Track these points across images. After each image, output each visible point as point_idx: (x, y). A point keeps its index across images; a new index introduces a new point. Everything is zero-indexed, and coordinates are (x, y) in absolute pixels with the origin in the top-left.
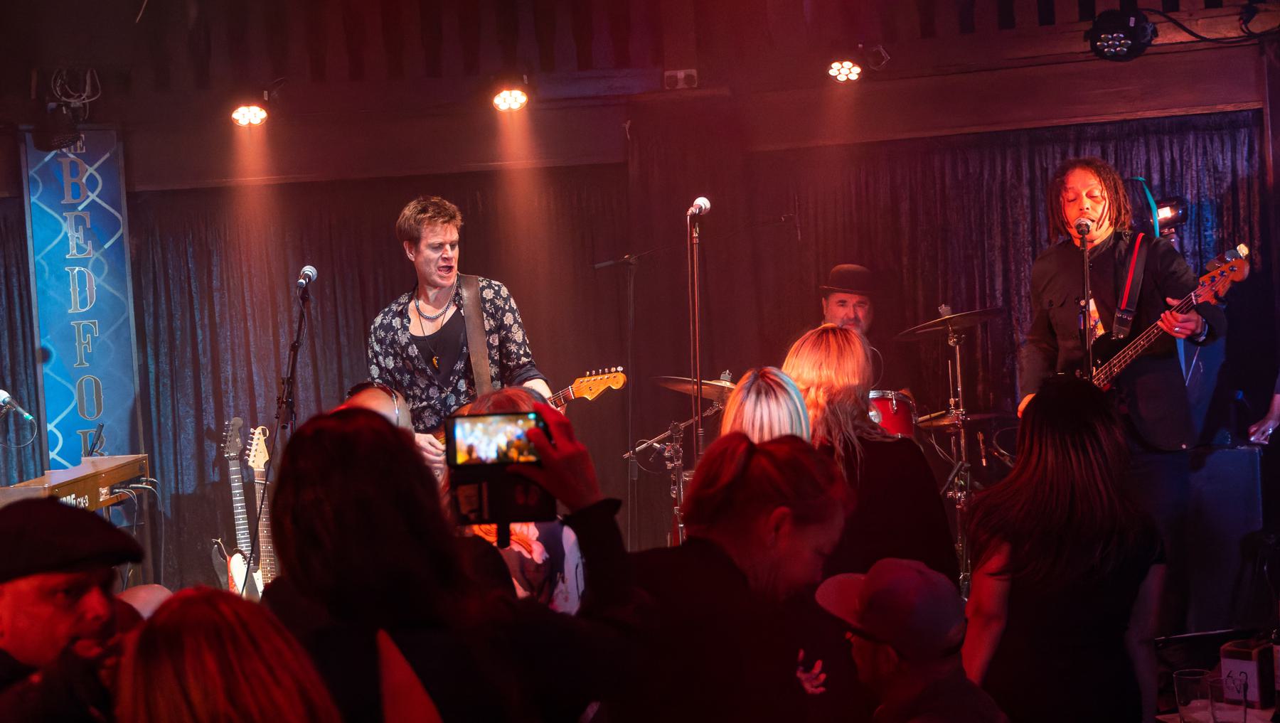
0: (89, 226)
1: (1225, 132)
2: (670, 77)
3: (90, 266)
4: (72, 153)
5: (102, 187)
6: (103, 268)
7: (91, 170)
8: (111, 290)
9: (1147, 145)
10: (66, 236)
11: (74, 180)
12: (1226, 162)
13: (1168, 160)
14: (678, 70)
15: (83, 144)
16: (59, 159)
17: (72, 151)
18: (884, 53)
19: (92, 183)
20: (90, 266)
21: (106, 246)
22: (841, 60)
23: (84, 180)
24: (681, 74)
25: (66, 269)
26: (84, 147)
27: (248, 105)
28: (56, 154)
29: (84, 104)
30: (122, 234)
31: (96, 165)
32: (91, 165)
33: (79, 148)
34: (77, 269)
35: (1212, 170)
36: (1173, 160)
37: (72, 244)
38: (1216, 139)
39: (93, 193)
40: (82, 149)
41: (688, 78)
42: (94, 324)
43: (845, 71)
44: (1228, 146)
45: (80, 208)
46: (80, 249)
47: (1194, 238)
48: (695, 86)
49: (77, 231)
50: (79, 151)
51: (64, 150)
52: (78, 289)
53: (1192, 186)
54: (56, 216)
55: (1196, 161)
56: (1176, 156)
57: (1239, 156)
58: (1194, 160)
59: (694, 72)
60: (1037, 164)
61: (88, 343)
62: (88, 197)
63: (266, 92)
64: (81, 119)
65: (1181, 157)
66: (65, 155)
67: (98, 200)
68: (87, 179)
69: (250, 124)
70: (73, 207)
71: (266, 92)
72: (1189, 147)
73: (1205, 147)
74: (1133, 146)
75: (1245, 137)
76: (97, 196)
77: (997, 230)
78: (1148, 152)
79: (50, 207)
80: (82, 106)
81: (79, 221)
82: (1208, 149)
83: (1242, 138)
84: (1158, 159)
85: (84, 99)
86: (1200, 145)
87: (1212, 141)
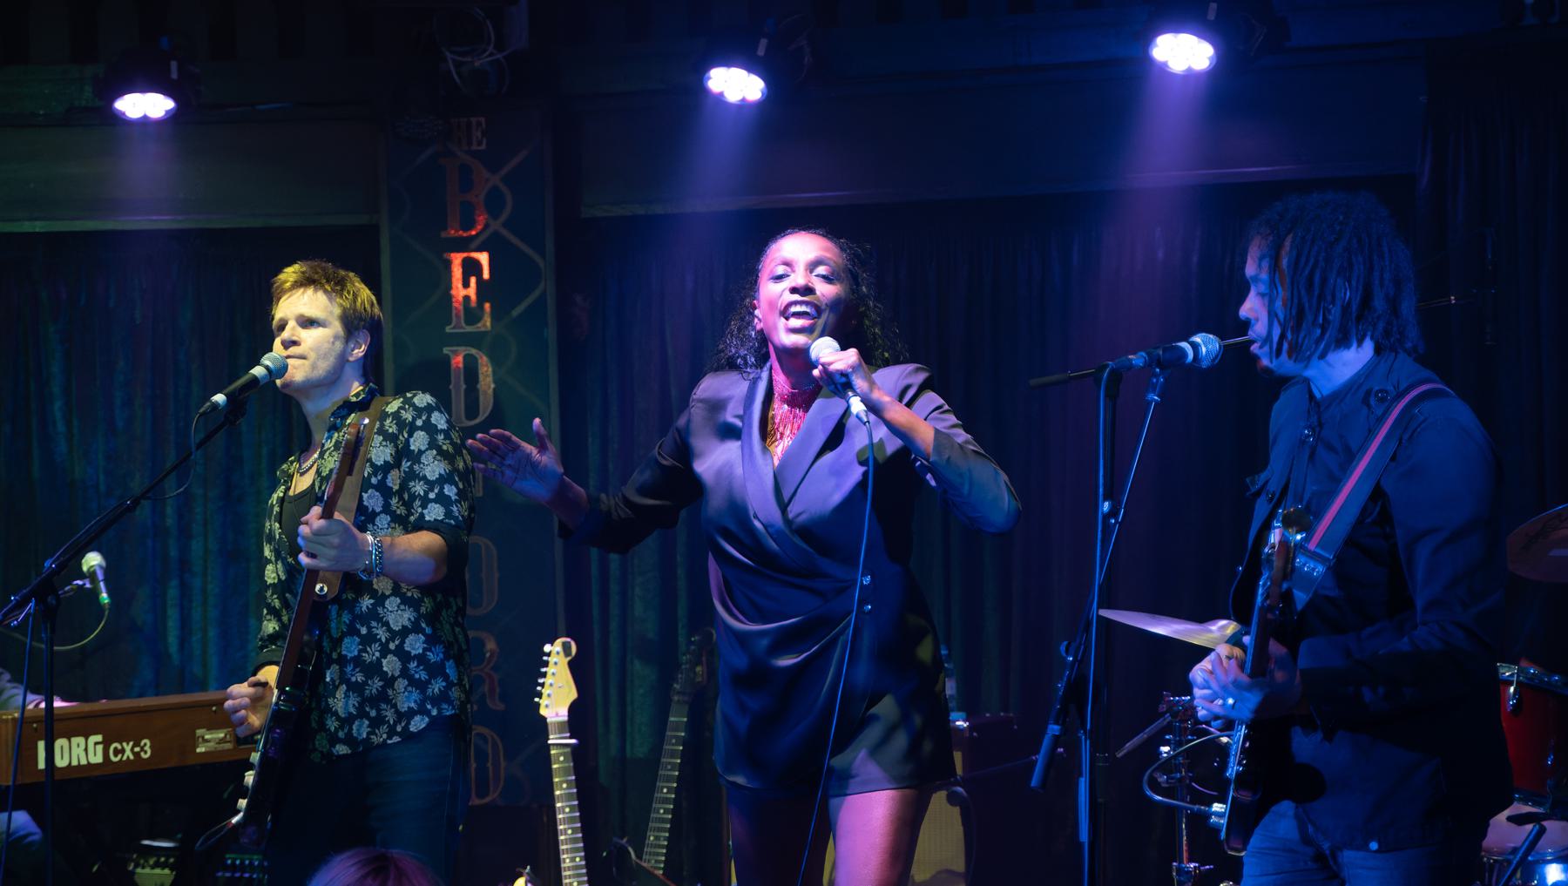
0: (486, 275)
19: (494, 204)
21: (515, 313)
25: (446, 350)
26: (485, 142)
27: (728, 65)
29: (498, 60)
30: (544, 292)
31: (504, 171)
39: (495, 216)
49: (466, 285)
50: (475, 147)
52: (451, 387)
63: (764, 42)
67: (505, 232)
69: (744, 100)
70: (462, 245)
71: (764, 42)
76: (505, 225)
81: (471, 268)
85: (490, 55)
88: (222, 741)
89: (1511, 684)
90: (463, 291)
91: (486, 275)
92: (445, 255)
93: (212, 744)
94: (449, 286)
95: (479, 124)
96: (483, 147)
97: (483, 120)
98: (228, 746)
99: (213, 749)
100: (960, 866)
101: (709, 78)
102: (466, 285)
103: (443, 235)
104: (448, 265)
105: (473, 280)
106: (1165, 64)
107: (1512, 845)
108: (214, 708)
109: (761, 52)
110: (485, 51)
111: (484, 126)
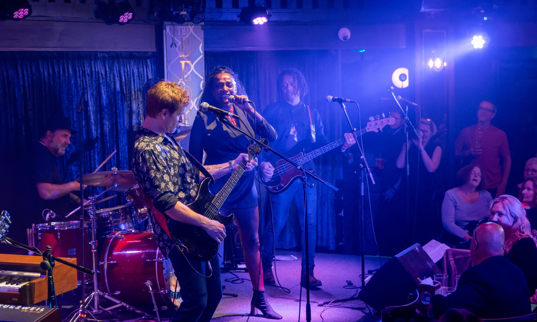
9: (119, 63)
44: (145, 67)
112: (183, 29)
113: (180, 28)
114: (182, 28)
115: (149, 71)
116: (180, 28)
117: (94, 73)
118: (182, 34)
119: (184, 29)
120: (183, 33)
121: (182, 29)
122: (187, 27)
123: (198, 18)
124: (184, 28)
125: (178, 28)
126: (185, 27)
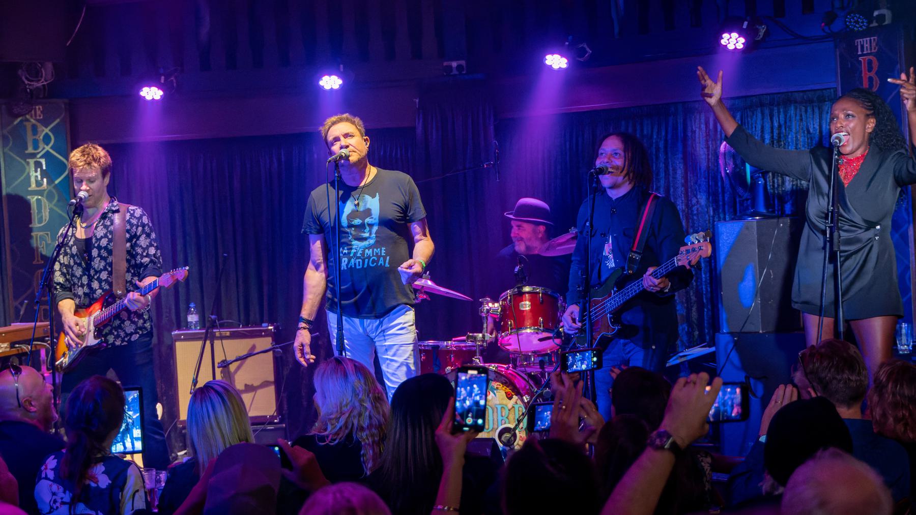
0: (44, 168)
1: (815, 104)
2: (446, 66)
3: (45, 195)
4: (34, 119)
5: (54, 144)
6: (54, 197)
7: (47, 130)
8: (61, 212)
9: (763, 114)
10: (29, 177)
11: (35, 137)
12: (815, 126)
13: (776, 124)
14: (452, 61)
15: (41, 112)
16: (25, 123)
17: (34, 118)
18: (588, 49)
19: (47, 139)
20: (45, 195)
21: (57, 182)
22: (553, 54)
23: (41, 137)
24: (454, 64)
26: (42, 115)
28: (21, 121)
29: (44, 85)
30: (68, 173)
32: (46, 127)
33: (38, 114)
34: (36, 197)
35: (806, 132)
36: (780, 126)
37: (33, 180)
38: (809, 110)
39: (47, 145)
40: (40, 116)
41: (459, 67)
42: (47, 234)
43: (556, 61)
45: (39, 156)
46: (39, 184)
47: (793, 181)
48: (464, 72)
49: (36, 171)
50: (38, 118)
51: (28, 116)
53: (793, 143)
54: (23, 162)
55: (794, 125)
56: (782, 122)
57: (824, 121)
58: (794, 124)
59: (463, 63)
60: (689, 128)
61: (43, 247)
62: (44, 149)
64: (41, 96)
65: (786, 122)
66: (28, 120)
67: (51, 151)
68: (44, 137)
70: (33, 156)
71: (163, 78)
72: (791, 115)
73: (801, 116)
74: (753, 115)
75: (829, 107)
76: (51, 148)
77: (662, 175)
78: (763, 119)
79: (18, 156)
80: (42, 87)
81: (38, 165)
82: (803, 117)
83: (827, 108)
84: (770, 124)
85: (43, 82)
86: (798, 115)
87: (806, 111)
88: (6, 348)
89: (539, 293)
90: (35, 175)
91: (44, 168)
92: (28, 160)
93: (3, 349)
94: (29, 174)
95: (39, 109)
96: (42, 117)
97: (41, 107)
98: (8, 349)
99: (3, 351)
100: (271, 378)
101: (142, 91)
102: (36, 171)
103: (27, 152)
104: (28, 163)
105: (39, 169)
106: (323, 87)
107: (533, 349)
108: (3, 335)
109: (162, 81)
110: (39, 80)
111: (41, 109)
112: (865, 44)
113: (860, 41)
114: (863, 41)
115: (826, 123)
116: (860, 41)
117: (712, 133)
118: (865, 52)
119: (867, 43)
120: (865, 49)
121: (863, 43)
122: (872, 38)
123: (857, 22)
124: (867, 40)
125: (857, 42)
126: (868, 39)
